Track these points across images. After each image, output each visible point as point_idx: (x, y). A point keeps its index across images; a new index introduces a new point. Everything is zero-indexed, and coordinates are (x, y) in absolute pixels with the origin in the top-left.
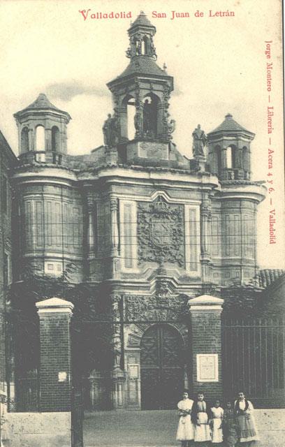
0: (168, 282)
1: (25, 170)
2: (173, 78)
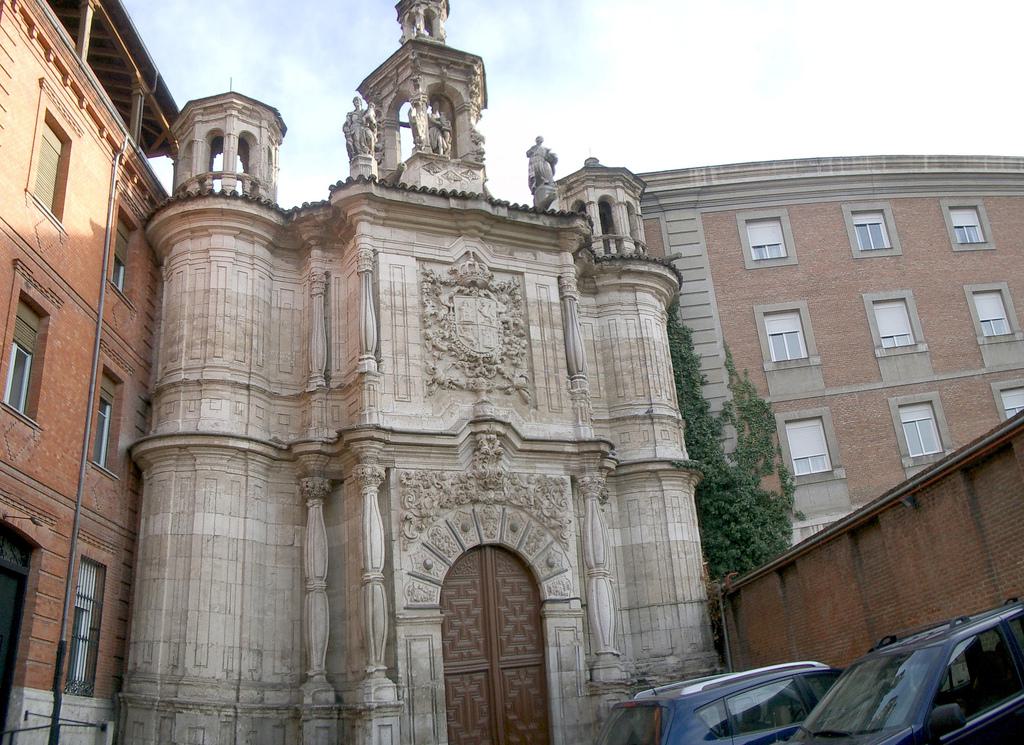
0: (499, 435)
2: (477, 59)
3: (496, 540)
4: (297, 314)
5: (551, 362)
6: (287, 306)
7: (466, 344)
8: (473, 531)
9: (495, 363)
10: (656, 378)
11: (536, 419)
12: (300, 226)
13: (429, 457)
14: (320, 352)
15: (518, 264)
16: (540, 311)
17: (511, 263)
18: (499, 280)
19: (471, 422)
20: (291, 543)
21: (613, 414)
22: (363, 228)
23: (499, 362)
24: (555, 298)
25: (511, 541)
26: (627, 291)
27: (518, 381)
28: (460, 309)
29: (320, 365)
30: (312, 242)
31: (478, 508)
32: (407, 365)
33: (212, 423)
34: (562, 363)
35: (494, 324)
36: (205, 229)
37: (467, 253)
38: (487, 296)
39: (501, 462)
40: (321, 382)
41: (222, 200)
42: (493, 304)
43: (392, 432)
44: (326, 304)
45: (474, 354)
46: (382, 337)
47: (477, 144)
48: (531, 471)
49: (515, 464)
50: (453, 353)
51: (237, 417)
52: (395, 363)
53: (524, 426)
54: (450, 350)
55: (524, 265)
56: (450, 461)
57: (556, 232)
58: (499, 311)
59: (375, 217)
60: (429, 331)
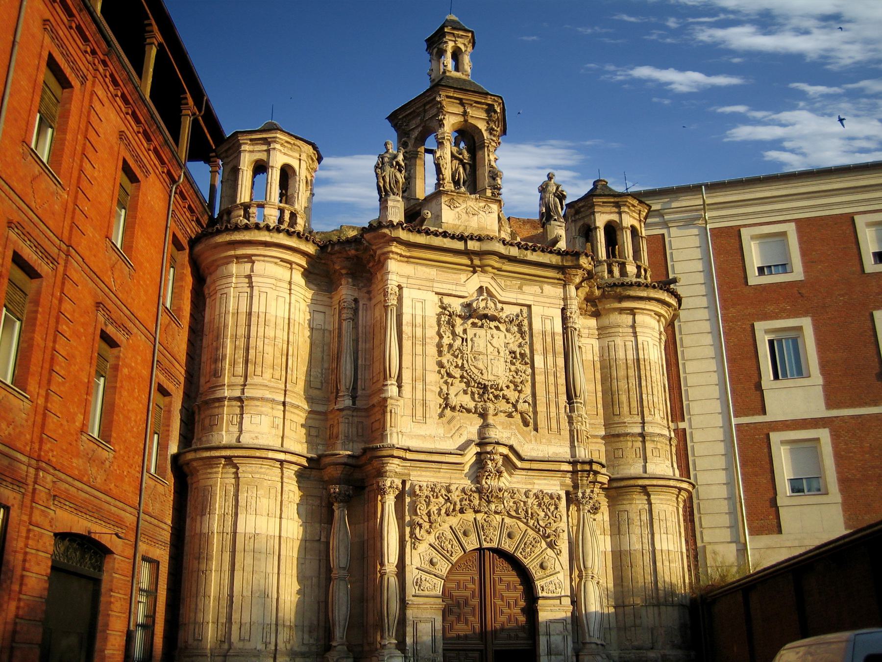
1: (227, 230)
3: (494, 545)
4: (327, 334)
6: (319, 327)
7: (475, 371)
8: (473, 537)
9: (502, 390)
10: (650, 397)
11: (536, 440)
12: (333, 257)
13: (439, 472)
14: (348, 373)
15: (526, 297)
16: (544, 340)
17: (521, 296)
20: (317, 538)
21: (608, 431)
22: (393, 265)
23: (505, 388)
24: (559, 328)
25: (508, 546)
26: (627, 314)
27: (522, 406)
28: (472, 340)
29: (348, 384)
30: (344, 272)
31: (479, 516)
32: (424, 390)
33: (253, 435)
34: (562, 389)
35: (502, 354)
37: (481, 288)
38: (497, 328)
39: (502, 479)
40: (348, 402)
41: (266, 233)
42: (502, 335)
43: (408, 450)
44: (356, 327)
46: (404, 365)
47: (494, 179)
48: (530, 487)
49: (515, 480)
51: (274, 431)
52: (414, 388)
53: (526, 446)
55: (531, 298)
56: (457, 475)
57: (561, 269)
59: (401, 255)
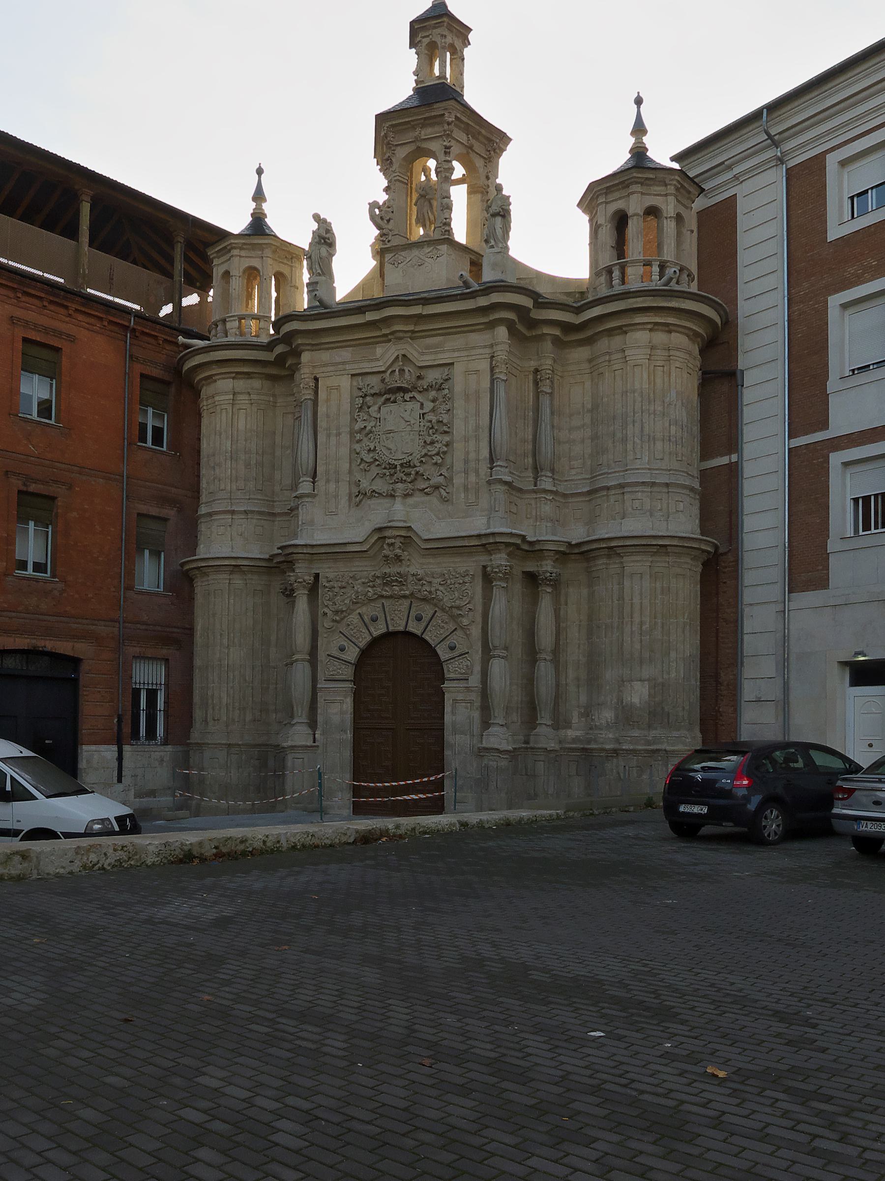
5: (472, 456)
9: (415, 466)
18: (432, 376)
19: (375, 529)
27: (437, 480)
36: (210, 377)
37: (397, 357)
45: (393, 462)
50: (378, 463)
54: (376, 460)
58: (422, 412)
60: (357, 447)
